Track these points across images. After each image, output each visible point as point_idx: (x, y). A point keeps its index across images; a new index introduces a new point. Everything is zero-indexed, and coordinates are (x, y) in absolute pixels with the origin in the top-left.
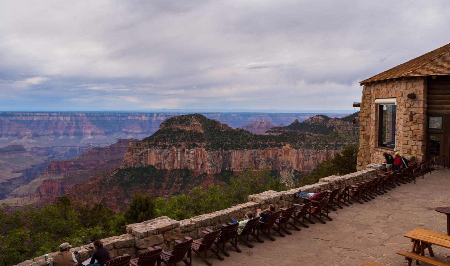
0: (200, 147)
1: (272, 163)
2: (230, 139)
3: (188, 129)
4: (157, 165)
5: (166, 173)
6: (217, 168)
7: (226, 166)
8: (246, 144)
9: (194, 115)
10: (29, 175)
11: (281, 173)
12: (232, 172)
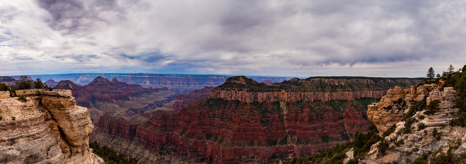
3: (238, 82)
4: (224, 98)
10: (169, 99)
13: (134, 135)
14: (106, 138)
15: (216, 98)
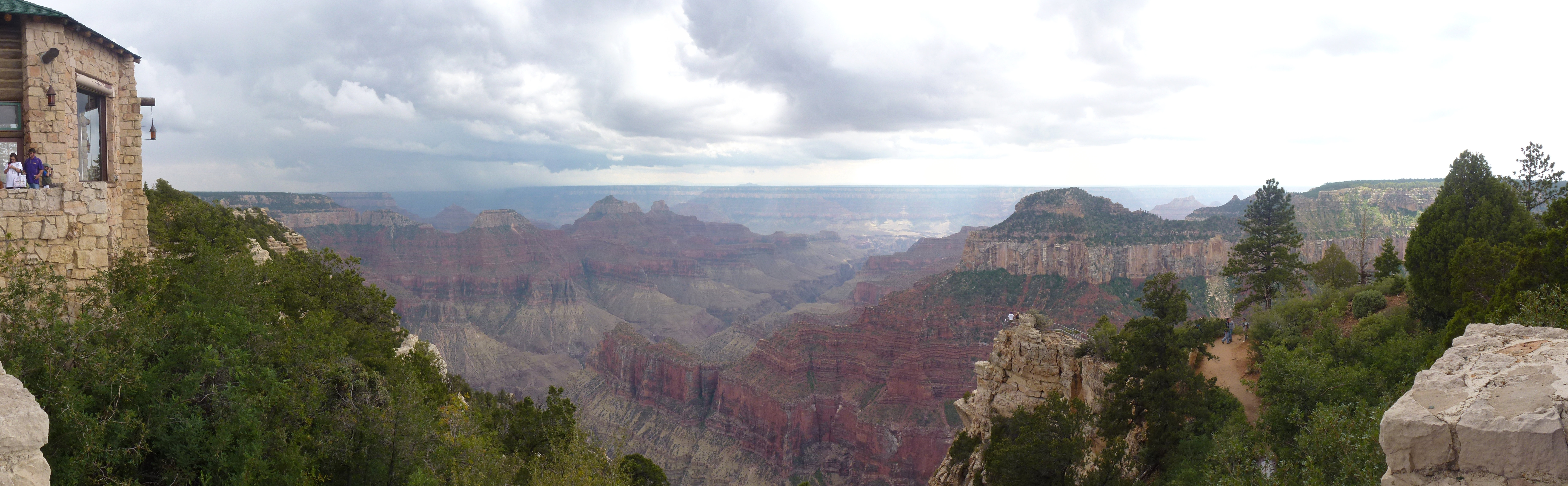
0: (1078, 240)
1: (1194, 265)
2: (1125, 228)
4: (1010, 267)
5: (1025, 281)
6: (1104, 273)
7: (1118, 271)
8: (1151, 236)
9: (1069, 190)
11: (1207, 280)
12: (1129, 280)
13: (710, 403)
14: (621, 413)
15: (982, 268)
